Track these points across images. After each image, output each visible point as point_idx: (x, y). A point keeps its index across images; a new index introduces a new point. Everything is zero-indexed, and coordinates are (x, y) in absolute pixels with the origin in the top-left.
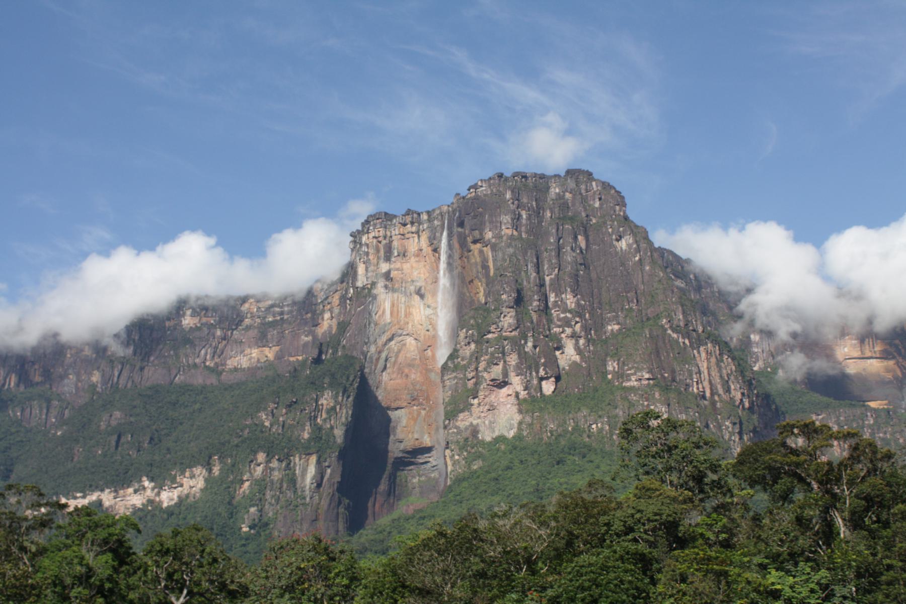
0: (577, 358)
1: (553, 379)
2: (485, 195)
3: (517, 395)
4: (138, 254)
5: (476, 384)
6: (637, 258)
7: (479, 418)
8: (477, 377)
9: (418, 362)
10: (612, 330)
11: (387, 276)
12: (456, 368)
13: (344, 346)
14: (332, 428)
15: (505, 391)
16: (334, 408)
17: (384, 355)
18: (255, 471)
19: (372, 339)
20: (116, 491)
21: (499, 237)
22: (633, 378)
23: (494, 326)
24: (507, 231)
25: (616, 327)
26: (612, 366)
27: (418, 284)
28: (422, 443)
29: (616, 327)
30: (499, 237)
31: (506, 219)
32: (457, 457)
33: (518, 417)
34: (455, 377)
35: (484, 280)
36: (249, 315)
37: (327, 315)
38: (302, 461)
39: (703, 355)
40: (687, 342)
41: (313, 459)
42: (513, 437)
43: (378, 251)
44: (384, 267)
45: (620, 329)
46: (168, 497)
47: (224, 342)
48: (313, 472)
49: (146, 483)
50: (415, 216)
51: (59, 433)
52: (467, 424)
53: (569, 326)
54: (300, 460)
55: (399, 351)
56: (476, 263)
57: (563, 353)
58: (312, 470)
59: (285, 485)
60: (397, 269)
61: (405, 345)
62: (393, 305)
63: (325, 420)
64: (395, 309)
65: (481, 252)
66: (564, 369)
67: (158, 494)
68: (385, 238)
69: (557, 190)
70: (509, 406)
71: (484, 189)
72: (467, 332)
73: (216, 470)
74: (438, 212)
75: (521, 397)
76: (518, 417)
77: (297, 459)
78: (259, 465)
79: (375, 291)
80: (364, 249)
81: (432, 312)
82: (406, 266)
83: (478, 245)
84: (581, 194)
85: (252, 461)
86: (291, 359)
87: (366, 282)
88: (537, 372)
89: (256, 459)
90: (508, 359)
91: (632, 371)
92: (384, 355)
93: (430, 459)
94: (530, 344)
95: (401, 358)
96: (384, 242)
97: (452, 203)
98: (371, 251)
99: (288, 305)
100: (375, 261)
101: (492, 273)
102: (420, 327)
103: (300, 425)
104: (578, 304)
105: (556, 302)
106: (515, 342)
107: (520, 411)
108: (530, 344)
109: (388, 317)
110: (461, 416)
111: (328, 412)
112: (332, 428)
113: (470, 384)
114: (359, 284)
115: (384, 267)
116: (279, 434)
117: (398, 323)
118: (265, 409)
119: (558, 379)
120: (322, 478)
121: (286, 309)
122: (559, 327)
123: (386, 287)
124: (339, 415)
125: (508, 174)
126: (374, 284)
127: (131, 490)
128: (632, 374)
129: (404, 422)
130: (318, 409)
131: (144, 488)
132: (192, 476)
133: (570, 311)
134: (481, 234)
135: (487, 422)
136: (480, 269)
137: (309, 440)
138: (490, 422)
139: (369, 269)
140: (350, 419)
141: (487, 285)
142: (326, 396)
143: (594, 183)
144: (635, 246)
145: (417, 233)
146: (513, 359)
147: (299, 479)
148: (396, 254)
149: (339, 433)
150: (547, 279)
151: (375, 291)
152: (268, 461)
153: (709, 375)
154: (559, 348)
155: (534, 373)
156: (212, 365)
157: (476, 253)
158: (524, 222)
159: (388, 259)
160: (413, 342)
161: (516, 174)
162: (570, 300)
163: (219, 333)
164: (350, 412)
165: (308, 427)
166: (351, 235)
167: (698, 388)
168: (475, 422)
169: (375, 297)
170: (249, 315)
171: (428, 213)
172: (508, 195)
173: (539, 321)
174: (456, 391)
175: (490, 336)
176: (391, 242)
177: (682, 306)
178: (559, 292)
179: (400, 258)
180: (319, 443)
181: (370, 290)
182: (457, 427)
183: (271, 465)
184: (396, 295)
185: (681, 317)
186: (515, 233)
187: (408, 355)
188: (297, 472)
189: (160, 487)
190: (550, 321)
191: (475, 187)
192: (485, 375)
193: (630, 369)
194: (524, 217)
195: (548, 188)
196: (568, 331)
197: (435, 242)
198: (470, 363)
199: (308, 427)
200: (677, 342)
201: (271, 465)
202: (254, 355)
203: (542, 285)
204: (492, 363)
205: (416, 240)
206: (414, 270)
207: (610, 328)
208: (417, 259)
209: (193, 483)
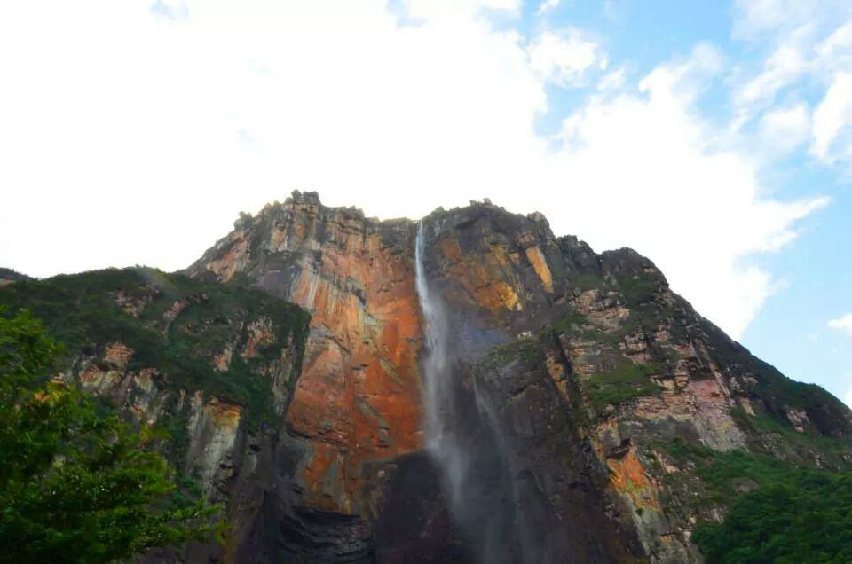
9: (341, 379)
11: (318, 256)
28: (336, 505)
35: (520, 286)
38: (209, 409)
44: (314, 245)
54: (205, 403)
56: (500, 267)
62: (320, 291)
64: (323, 298)
70: (721, 412)
78: (104, 368)
81: (375, 324)
85: (88, 352)
93: (339, 541)
102: (354, 335)
117: (325, 315)
147: (194, 444)
151: (299, 262)
160: (338, 351)
165: (228, 354)
166: (242, 214)
168: (680, 418)
169: (299, 269)
184: (326, 282)
187: (329, 366)
188: (191, 427)
199: (228, 354)
205: (361, 239)
208: (358, 259)
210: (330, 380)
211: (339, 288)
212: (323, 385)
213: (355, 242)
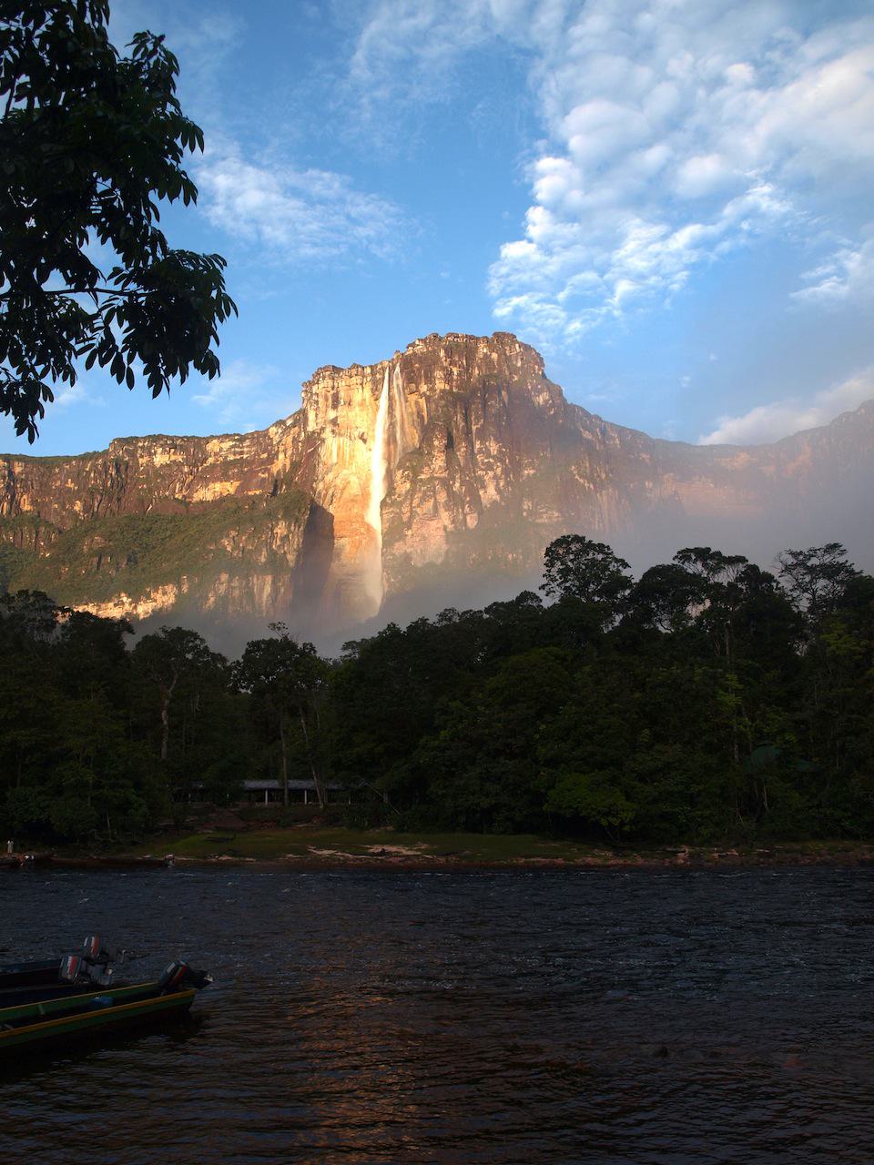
0: (498, 498)
1: (476, 515)
2: (422, 353)
3: (445, 528)
4: (210, 366)
5: (411, 517)
6: (552, 413)
7: (412, 546)
8: (411, 511)
10: (528, 474)
11: (334, 422)
12: (393, 503)
13: (296, 483)
14: (285, 553)
15: (434, 524)
16: (287, 536)
17: (330, 492)
18: (219, 590)
19: (320, 477)
20: (97, 605)
21: (432, 390)
22: (545, 516)
23: (427, 468)
24: (440, 385)
25: (532, 472)
26: (527, 505)
27: (362, 430)
29: (532, 472)
30: (432, 390)
31: (438, 374)
32: (392, 580)
33: (445, 547)
34: (392, 512)
35: (419, 428)
36: (212, 454)
37: (281, 456)
39: (605, 498)
40: (592, 486)
41: (269, 579)
42: (442, 564)
43: (327, 400)
44: (332, 414)
45: (535, 474)
46: (143, 609)
47: (191, 477)
48: (269, 591)
49: (125, 599)
50: (360, 369)
51: (47, 555)
52: (402, 552)
53: (492, 469)
54: (258, 579)
55: (344, 489)
57: (486, 492)
58: (268, 589)
59: (245, 602)
60: (344, 417)
61: (349, 483)
62: (339, 448)
63: (279, 546)
65: (417, 403)
66: (486, 507)
67: (135, 608)
68: (333, 388)
69: (485, 351)
71: (420, 348)
72: (403, 472)
73: (185, 589)
74: (379, 367)
75: (448, 530)
76: (445, 547)
77: (255, 579)
79: (323, 436)
80: (315, 397)
82: (351, 414)
83: (413, 398)
84: (505, 354)
86: (250, 493)
87: (316, 427)
88: (463, 509)
89: (220, 579)
90: (438, 497)
91: (544, 510)
92: (330, 492)
94: (457, 485)
95: (346, 495)
96: (332, 392)
97: (393, 359)
98: (321, 400)
99: (247, 447)
100: (324, 409)
101: (426, 423)
103: (258, 550)
104: (500, 451)
105: (481, 449)
106: (446, 484)
107: (447, 542)
108: (457, 485)
109: (334, 459)
110: (397, 545)
111: (282, 539)
112: (285, 553)
113: (405, 518)
114: (310, 429)
115: (332, 414)
116: (239, 558)
118: (228, 536)
119: (480, 514)
120: (277, 595)
121: (245, 450)
122: (482, 470)
123: (333, 431)
124: (291, 543)
125: (442, 334)
126: (323, 429)
127: (111, 605)
128: (543, 513)
129: (348, 548)
130: (273, 536)
131: (123, 603)
132: (165, 593)
133: (493, 457)
134: (417, 387)
135: (419, 551)
136: (415, 418)
137: (265, 564)
138: (421, 551)
139: (319, 416)
140: (301, 546)
141: (422, 432)
142: (280, 526)
143: (517, 345)
144: (550, 402)
145: (362, 384)
146: (442, 497)
148: (342, 403)
149: (291, 557)
150: (474, 428)
151: (323, 436)
152: (230, 581)
153: (609, 515)
154: (484, 487)
155: (460, 510)
156: (180, 498)
157: (413, 403)
158: (455, 377)
159: (335, 407)
160: (357, 481)
161: (450, 335)
162: (494, 447)
163: (186, 469)
164: (301, 540)
165: (264, 553)
167: (599, 526)
168: (408, 551)
169: (323, 441)
170: (212, 454)
171: (371, 367)
172: (442, 353)
173: (466, 465)
174: (393, 523)
175: (423, 476)
176: (338, 393)
177: (589, 455)
178: (483, 440)
179: (346, 407)
180: (276, 564)
181: (319, 434)
182: (394, 555)
183: (233, 584)
184: (341, 439)
185: (588, 465)
186: (447, 387)
187: (352, 492)
189: (136, 601)
190: (475, 463)
191: (413, 345)
192: (418, 510)
193: (543, 508)
194: (455, 373)
195: (477, 348)
196: (491, 474)
197: (377, 393)
198: (405, 500)
199: (264, 553)
200: (583, 485)
201: (233, 584)
202: (217, 490)
203: (468, 432)
204: (423, 500)
205: (360, 391)
206: (356, 417)
207: (526, 472)
209: (164, 598)
210: (353, 500)
211: (351, 439)
212: (350, 505)
213: (358, 396)
